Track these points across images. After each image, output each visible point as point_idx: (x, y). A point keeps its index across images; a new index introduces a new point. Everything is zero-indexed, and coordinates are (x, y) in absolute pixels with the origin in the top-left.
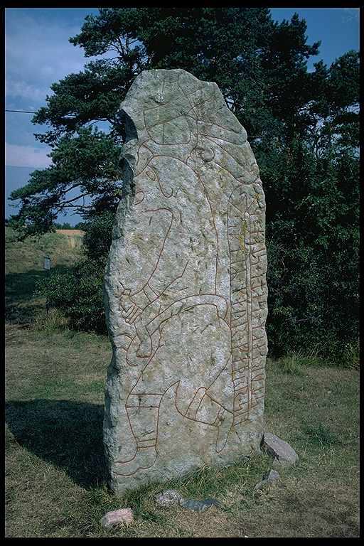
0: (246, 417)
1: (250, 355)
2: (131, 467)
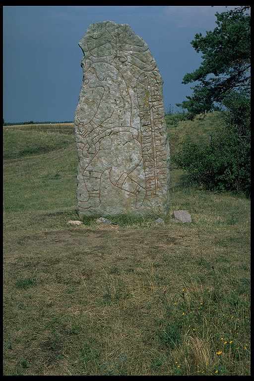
0: (155, 193)
1: (155, 160)
2: (86, 205)
